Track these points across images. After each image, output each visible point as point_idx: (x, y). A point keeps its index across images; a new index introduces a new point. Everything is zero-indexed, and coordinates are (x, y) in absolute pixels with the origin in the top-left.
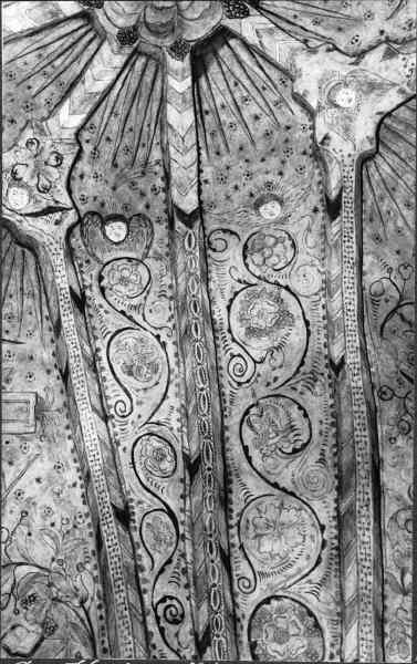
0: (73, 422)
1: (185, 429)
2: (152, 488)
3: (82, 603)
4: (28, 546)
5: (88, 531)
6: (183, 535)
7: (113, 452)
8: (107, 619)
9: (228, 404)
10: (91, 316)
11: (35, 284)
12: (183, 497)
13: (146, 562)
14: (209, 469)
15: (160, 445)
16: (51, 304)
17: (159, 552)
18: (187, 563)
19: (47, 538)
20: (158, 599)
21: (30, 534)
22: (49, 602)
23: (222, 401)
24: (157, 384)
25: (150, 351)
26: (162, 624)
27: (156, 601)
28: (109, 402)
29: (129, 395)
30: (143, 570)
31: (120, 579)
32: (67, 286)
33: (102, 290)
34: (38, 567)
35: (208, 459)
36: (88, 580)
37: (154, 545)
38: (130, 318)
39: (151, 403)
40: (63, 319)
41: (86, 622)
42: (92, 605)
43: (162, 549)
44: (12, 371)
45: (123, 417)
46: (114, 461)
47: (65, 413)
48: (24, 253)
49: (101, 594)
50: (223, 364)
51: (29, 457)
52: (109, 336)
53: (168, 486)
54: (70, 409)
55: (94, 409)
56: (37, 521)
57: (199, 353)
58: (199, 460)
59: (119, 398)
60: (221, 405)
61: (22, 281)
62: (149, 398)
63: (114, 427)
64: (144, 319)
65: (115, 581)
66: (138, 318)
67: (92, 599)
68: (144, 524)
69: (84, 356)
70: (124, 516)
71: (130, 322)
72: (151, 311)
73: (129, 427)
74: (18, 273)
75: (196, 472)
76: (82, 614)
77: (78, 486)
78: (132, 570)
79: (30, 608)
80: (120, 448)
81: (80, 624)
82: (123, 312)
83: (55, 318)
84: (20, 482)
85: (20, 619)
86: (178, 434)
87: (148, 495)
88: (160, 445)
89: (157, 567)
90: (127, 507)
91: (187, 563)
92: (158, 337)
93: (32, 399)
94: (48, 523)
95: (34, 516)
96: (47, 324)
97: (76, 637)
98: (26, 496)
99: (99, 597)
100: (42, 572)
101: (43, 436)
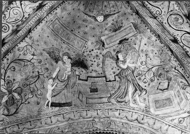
1: (180, 8)
2: (179, 29)
3: (175, 69)
4: (152, 62)
5: (167, 50)
7: (163, 26)
8: (185, 69)
15: (175, 16)
19: (156, 58)
21: (151, 59)
22: (166, 73)
28: (154, 13)
29: (158, 8)
30: (188, 52)
31: (183, 57)
34: (158, 66)
36: (174, 62)
37: (188, 44)
41: (179, 73)
42: (178, 68)
45: (160, 15)
47: (143, 23)
51: (139, 40)
53: (184, 26)
54: (144, 21)
55: (151, 17)
56: (151, 55)
62: (165, 5)
63: (159, 19)
67: (177, 66)
69: (140, 5)
70: (175, 41)
73: (163, 17)
76: (177, 71)
77: (157, 40)
78: (185, 53)
79: (161, 77)
80: (164, 24)
81: (177, 74)
84: (141, 47)
85: (160, 81)
86: (179, 11)
87: (179, 31)
88: (175, 16)
90: (174, 38)
93: (132, 24)
95: (149, 54)
97: (178, 78)
98: (144, 50)
99: (179, 65)
100: (159, 67)
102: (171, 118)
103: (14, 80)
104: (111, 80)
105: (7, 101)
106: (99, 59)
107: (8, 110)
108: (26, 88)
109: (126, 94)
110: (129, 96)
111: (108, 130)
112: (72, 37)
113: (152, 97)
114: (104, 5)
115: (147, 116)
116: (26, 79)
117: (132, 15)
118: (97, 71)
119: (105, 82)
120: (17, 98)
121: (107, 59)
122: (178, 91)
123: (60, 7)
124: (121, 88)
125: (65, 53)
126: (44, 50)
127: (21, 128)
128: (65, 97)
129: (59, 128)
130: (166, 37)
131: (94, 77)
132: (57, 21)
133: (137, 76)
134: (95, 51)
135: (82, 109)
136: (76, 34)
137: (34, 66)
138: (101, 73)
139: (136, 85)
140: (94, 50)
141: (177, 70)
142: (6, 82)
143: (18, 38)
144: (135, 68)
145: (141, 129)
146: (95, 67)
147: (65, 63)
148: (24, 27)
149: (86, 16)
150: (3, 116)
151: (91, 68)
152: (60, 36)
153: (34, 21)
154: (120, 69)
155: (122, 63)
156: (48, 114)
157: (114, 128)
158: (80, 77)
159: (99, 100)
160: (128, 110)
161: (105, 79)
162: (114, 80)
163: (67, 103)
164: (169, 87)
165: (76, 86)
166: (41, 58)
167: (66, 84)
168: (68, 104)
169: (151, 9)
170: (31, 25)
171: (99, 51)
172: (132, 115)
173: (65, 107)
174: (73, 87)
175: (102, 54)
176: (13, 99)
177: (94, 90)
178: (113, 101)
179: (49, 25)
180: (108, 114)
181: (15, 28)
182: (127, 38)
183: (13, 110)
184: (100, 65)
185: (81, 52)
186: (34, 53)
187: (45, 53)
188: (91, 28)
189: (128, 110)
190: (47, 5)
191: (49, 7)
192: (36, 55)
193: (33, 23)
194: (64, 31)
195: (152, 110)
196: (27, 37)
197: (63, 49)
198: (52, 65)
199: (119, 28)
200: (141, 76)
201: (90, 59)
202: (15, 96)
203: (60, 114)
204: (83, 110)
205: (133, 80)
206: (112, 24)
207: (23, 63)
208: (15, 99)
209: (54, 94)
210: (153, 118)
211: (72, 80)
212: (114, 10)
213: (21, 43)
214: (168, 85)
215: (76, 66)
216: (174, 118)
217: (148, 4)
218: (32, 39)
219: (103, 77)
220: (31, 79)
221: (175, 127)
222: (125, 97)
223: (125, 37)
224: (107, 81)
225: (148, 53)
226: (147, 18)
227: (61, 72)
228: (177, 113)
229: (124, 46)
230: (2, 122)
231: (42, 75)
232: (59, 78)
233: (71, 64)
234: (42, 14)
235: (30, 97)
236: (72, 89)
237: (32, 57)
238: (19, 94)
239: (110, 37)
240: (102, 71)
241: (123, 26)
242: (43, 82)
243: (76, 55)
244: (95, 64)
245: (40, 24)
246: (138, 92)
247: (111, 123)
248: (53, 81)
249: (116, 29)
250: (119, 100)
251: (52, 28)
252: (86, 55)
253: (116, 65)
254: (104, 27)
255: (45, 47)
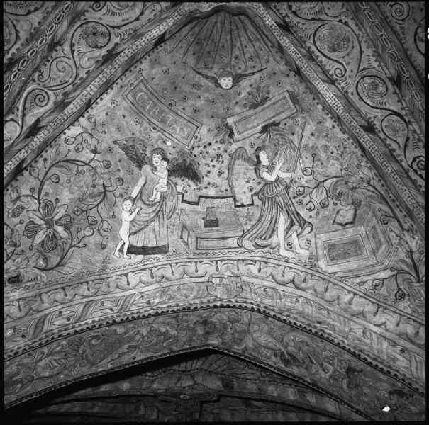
0: (315, 94)
1: (382, 64)
3: (369, 183)
6: (409, 121)
7: (347, 98)
8: (386, 184)
9: (401, 35)
10: (295, 32)
11: (255, 32)
12: (399, 101)
13: (394, 146)
14: (407, 78)
16: (270, 37)
17: (399, 137)
18: (418, 135)
20: (411, 161)
22: (350, 191)
23: (397, 35)
24: (353, 47)
25: (339, 32)
26: (419, 173)
27: (410, 164)
28: (330, 73)
30: (394, 150)
31: (384, 161)
32: (273, 23)
33: (295, 13)
35: (404, 72)
36: (366, 171)
38: (319, 19)
39: (355, 60)
40: (281, 42)
42: (375, 182)
43: (400, 135)
44: (268, 86)
45: (343, 76)
46: (349, 104)
47: (308, 93)
48: (239, 18)
49: (378, 175)
50: (388, 14)
52: (312, 37)
53: (388, 100)
55: (324, 81)
56: (323, 156)
57: (369, 15)
58: (399, 76)
59: (335, 68)
60: (398, 39)
61: (247, 34)
63: (340, 84)
64: (328, 16)
65: (382, 163)
66: (323, 17)
67: (373, 179)
68: (384, 128)
69: (304, 56)
70: (370, 129)
71: (319, 22)
72: (329, 9)
73: (349, 80)
74: (243, 32)
75: (400, 84)
76: (371, 189)
77: (336, 126)
80: (350, 94)
82: (313, 19)
83: (276, 45)
84: (303, 141)
85: (339, 206)
86: (380, 69)
87: (378, 110)
89: (402, 146)
90: (369, 123)
91: (418, 135)
92: (341, 21)
93: (287, 95)
94: (329, 153)
96: (274, 50)
98: (311, 145)
99: (377, 176)
100: (338, 179)
101: (302, 111)
102: (358, 280)
103: (57, 200)
104: (245, 204)
105: (43, 241)
106: (223, 161)
107: (46, 259)
108: (80, 217)
109: (273, 230)
110: (279, 237)
111: (237, 302)
112: (171, 117)
113: (323, 237)
114: (234, 55)
115: (312, 275)
116: (81, 200)
117: (288, 75)
118: (218, 184)
119: (233, 206)
120: (62, 235)
121: (237, 162)
122: (374, 227)
123: (148, 58)
124: (263, 219)
125: (156, 149)
126: (115, 142)
127: (70, 295)
128: (156, 236)
129: (142, 296)
130: (352, 121)
131: (212, 198)
132: (141, 85)
133: (294, 198)
134: (215, 146)
135: (188, 260)
136: (181, 114)
137: (95, 174)
138: (227, 190)
139: (293, 214)
140: (213, 144)
141: (371, 186)
142: (41, 206)
143: (65, 118)
144: (292, 180)
145: (301, 300)
146: (213, 178)
147: (156, 168)
148: (78, 96)
149: (198, 76)
150: (37, 271)
151: (206, 179)
152: (147, 116)
153: (96, 84)
154: (263, 183)
155: (266, 170)
156: (122, 269)
157: (249, 296)
158: (185, 196)
159: (222, 243)
160: (276, 262)
161: (233, 202)
162: (251, 203)
163: (157, 247)
164: (357, 219)
165: (177, 214)
166: (108, 157)
167: (158, 209)
168: (162, 250)
169: (325, 66)
170: (92, 93)
171: (222, 147)
172: (284, 272)
173: (156, 256)
174: (171, 217)
175: (228, 151)
176: (55, 237)
177: (212, 223)
178: (248, 244)
179: (125, 93)
180: (238, 270)
181: (60, 98)
182: (277, 122)
183: (55, 260)
184: (224, 173)
185: (187, 147)
186: (96, 147)
187: (117, 148)
188: (207, 100)
189: (276, 262)
190: (122, 54)
191: (126, 58)
192: (99, 153)
193: (95, 89)
194: (155, 105)
195: (322, 264)
196: (83, 117)
197: (153, 141)
198: (131, 172)
199: (261, 101)
200: (304, 197)
201: (204, 161)
202: (58, 233)
203: (145, 269)
204: (189, 262)
205: (286, 204)
206: (249, 94)
207: (74, 168)
208: (58, 238)
209: (134, 229)
210: (324, 279)
211: (170, 203)
212: (253, 65)
213: (72, 127)
214: (355, 215)
215: (177, 174)
216: (365, 279)
217: (320, 54)
218: (93, 120)
219: (230, 197)
220: (89, 200)
221: (367, 297)
222: (270, 237)
223: (273, 120)
224: (236, 206)
225: (317, 151)
226: (317, 83)
227: (149, 187)
228: (370, 269)
229: (270, 136)
230: (34, 283)
231: (110, 191)
232: (143, 198)
233: (167, 171)
234: (113, 71)
235: (87, 234)
236: (168, 219)
237: (92, 155)
238: (67, 229)
239: (243, 119)
240: (227, 184)
241: (271, 97)
242: (113, 205)
243: (178, 153)
244: (215, 171)
245: (108, 91)
246: (296, 227)
247: (244, 287)
248: (131, 204)
249: (256, 103)
250: (260, 242)
251: (131, 99)
252: (196, 153)
253: (254, 175)
254: (233, 99)
255: (118, 136)
